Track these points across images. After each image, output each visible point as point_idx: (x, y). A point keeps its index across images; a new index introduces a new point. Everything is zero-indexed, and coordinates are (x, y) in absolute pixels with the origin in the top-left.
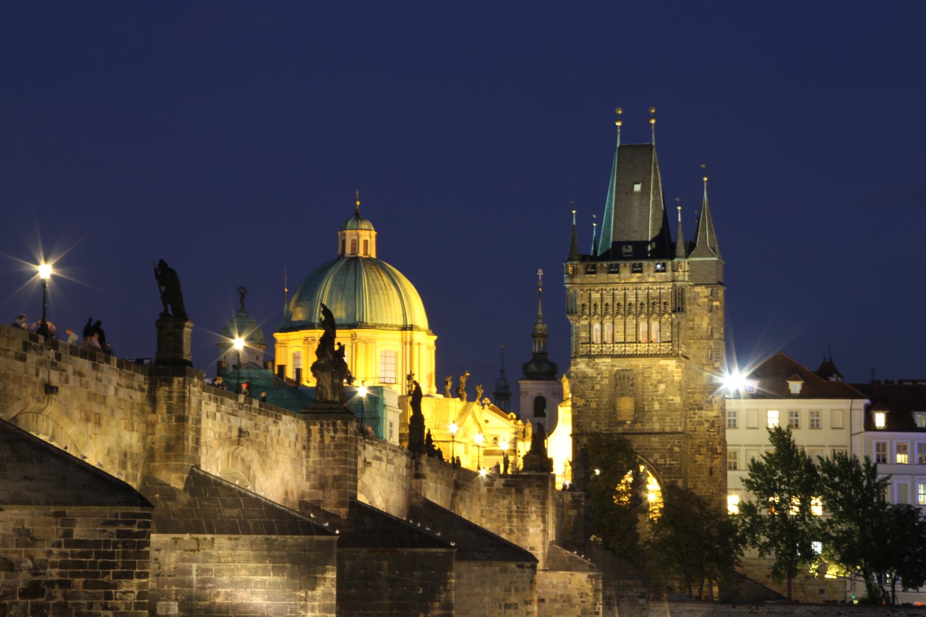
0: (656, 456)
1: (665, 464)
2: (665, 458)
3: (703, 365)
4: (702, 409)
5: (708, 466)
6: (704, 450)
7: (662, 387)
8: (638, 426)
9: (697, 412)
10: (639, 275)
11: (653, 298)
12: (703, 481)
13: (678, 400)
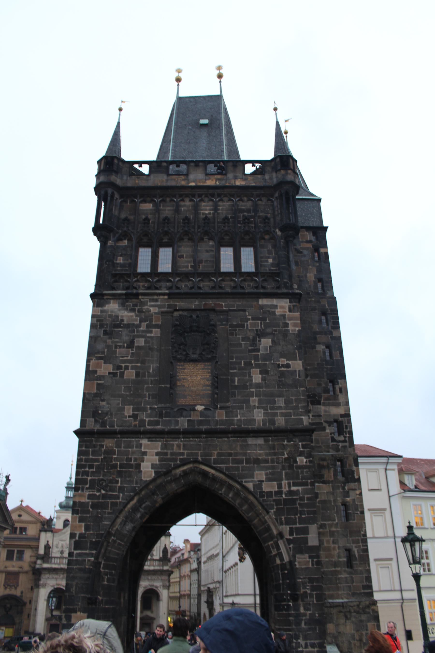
0: (260, 475)
1: (279, 493)
2: (279, 480)
3: (316, 333)
4: (319, 403)
5: (340, 500)
6: (329, 475)
7: (266, 342)
8: (220, 415)
9: (311, 407)
10: (219, 177)
11: (242, 211)
12: (332, 534)
13: (297, 365)
